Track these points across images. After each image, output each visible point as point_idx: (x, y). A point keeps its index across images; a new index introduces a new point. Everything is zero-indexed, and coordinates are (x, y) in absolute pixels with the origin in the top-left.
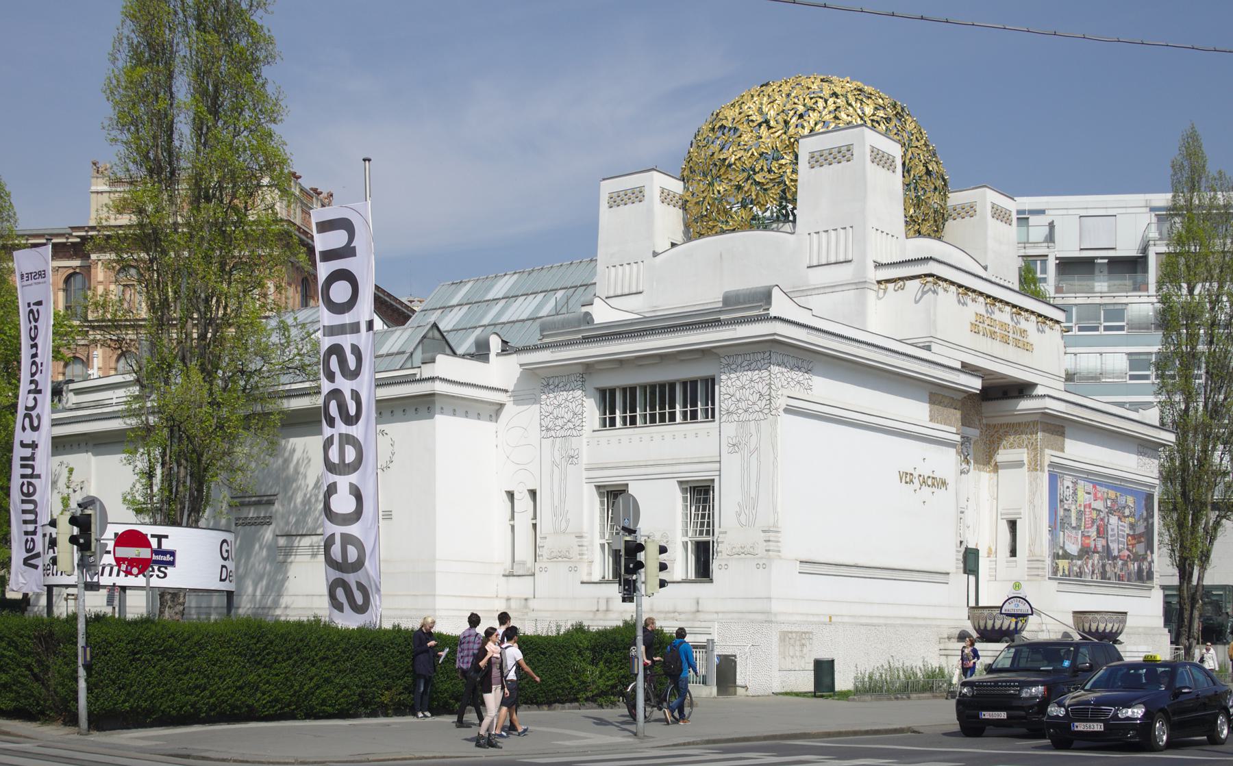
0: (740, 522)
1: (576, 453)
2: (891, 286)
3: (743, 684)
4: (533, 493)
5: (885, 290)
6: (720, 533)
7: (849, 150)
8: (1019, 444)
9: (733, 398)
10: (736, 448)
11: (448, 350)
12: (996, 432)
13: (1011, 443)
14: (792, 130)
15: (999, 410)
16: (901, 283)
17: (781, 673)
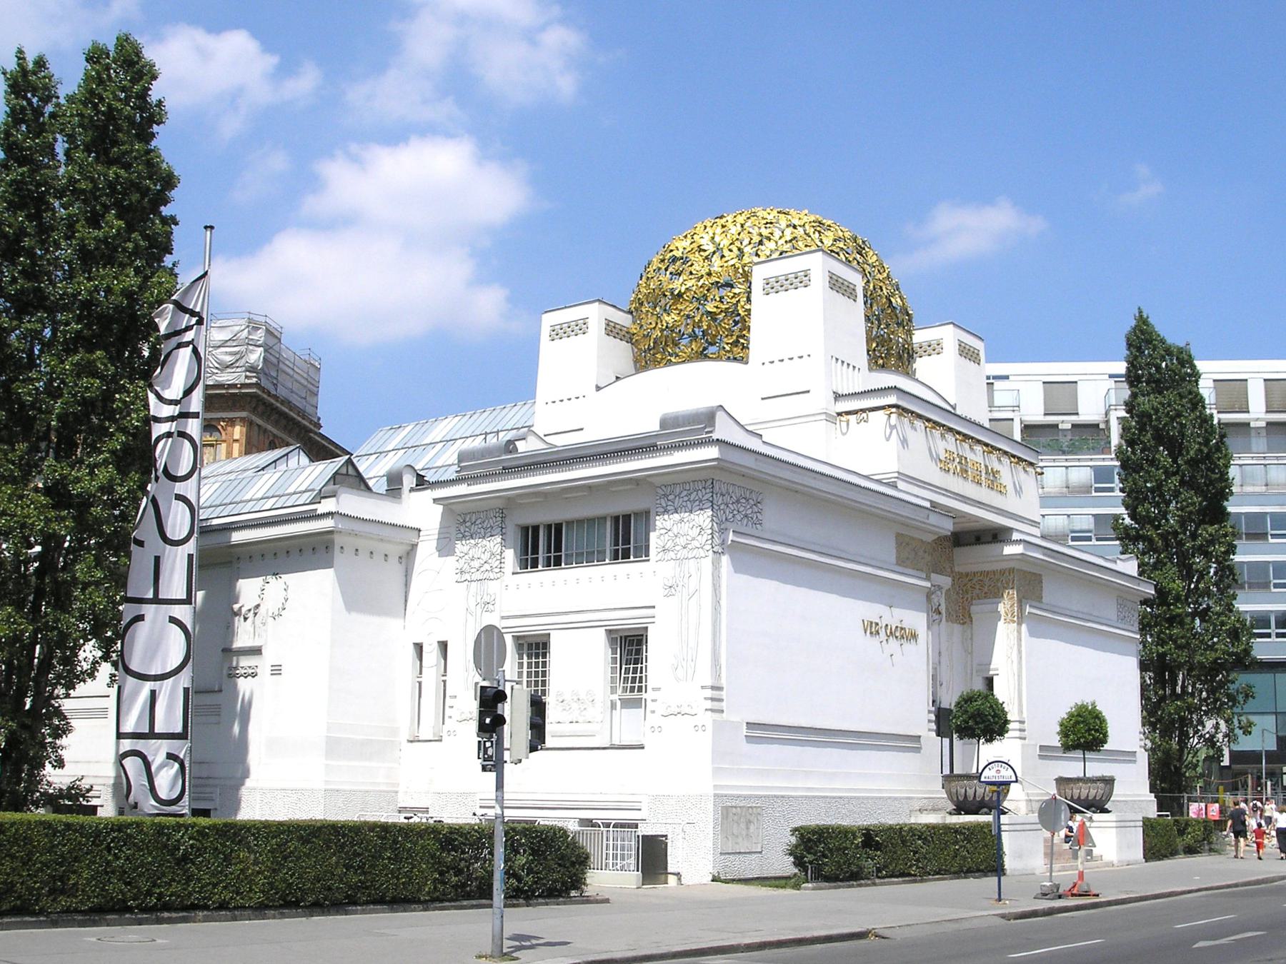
0: (678, 680)
1: (492, 599)
2: (852, 418)
3: (675, 871)
4: (444, 646)
5: (848, 422)
6: (654, 689)
7: (806, 276)
8: (995, 593)
9: (670, 533)
10: (673, 590)
11: (363, 487)
12: (970, 580)
13: (986, 593)
14: (746, 260)
15: (975, 559)
16: (864, 415)
17: (723, 857)
